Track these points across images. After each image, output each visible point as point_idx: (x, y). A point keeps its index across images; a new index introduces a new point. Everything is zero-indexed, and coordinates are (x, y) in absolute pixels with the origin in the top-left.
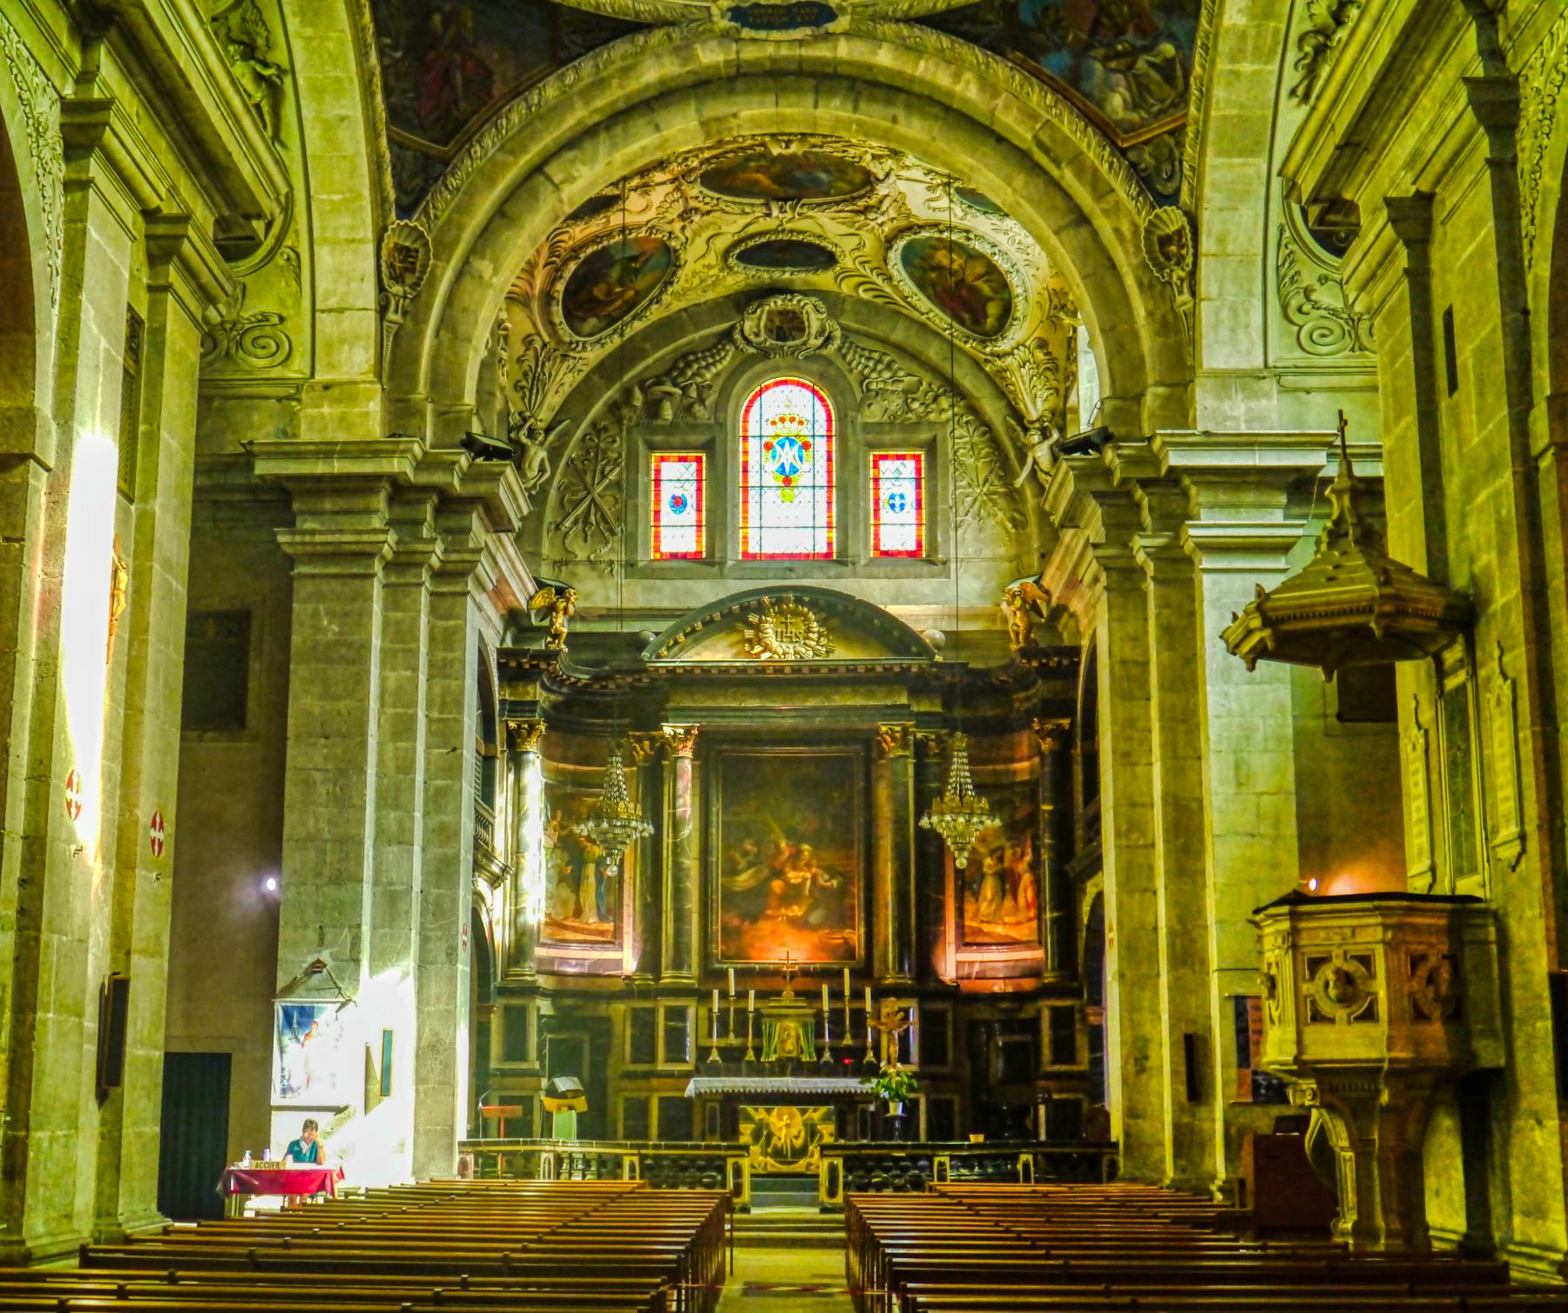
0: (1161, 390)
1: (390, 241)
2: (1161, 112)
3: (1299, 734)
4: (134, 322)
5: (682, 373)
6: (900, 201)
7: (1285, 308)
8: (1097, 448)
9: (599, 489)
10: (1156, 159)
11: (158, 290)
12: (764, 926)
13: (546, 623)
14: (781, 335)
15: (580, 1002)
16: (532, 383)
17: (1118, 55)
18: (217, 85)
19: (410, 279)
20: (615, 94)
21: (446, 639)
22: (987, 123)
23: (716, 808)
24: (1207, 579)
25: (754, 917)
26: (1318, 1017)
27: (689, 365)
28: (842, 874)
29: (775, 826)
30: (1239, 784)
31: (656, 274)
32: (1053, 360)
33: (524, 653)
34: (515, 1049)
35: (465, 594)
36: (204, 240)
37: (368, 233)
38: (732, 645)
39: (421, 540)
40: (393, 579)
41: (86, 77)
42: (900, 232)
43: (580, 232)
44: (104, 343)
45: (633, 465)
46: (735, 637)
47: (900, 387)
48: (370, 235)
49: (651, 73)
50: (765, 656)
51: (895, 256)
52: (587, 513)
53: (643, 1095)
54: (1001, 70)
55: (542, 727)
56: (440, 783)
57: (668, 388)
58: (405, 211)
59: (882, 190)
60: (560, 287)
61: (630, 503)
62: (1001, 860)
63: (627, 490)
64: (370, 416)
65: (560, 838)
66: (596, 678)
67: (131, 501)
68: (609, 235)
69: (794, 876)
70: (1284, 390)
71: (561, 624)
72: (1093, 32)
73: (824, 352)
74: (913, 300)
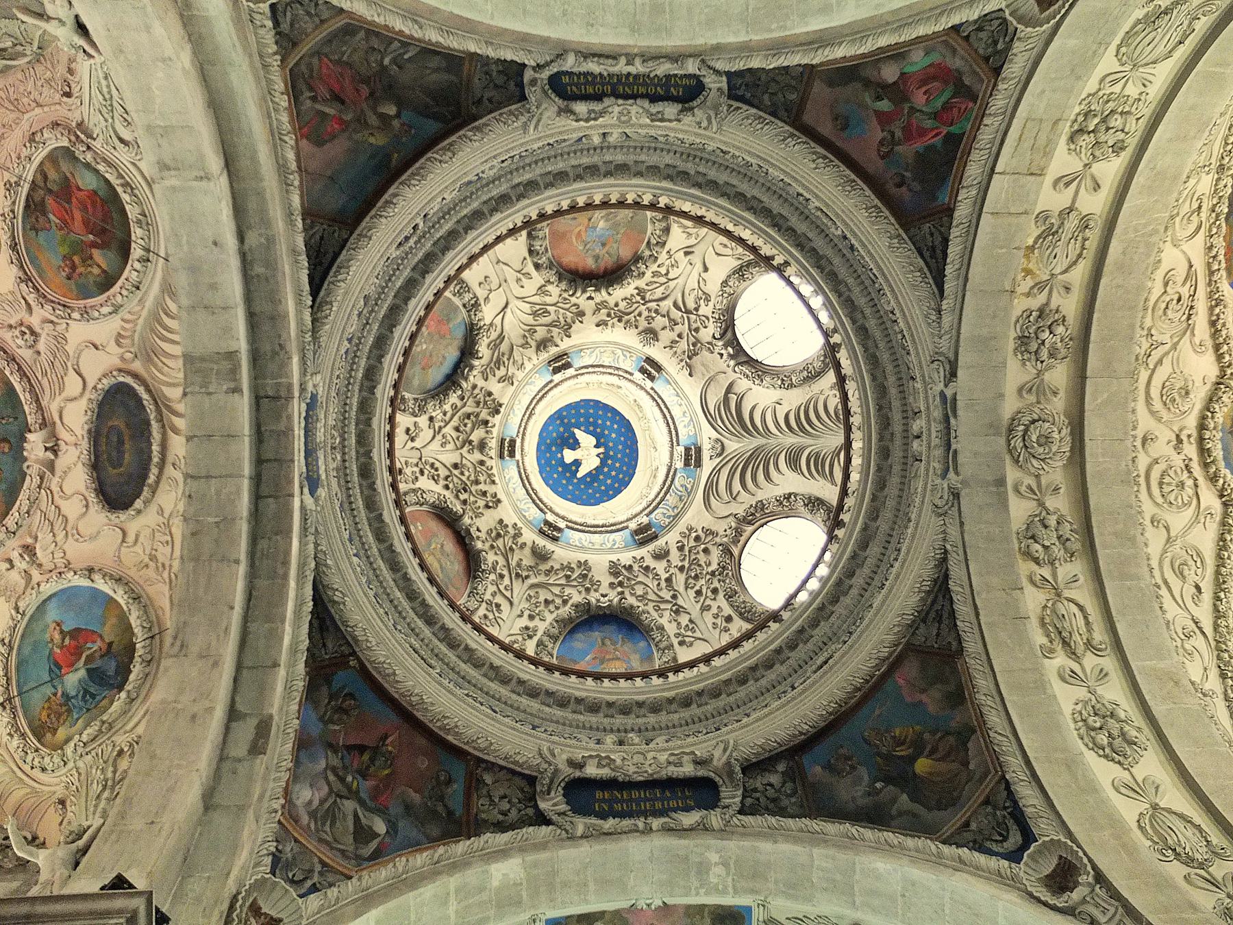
10: (294, 858)
22: (248, 662)
72: (349, 748)
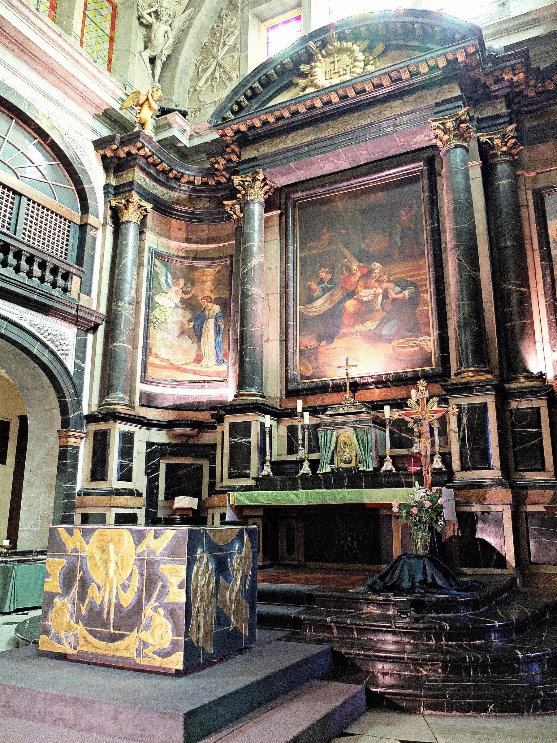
9: (221, 54)
12: (337, 343)
15: (190, 431)
23: (294, 247)
25: (329, 337)
28: (413, 284)
29: (347, 252)
45: (244, 31)
61: (243, 55)
65: (183, 301)
69: (365, 294)
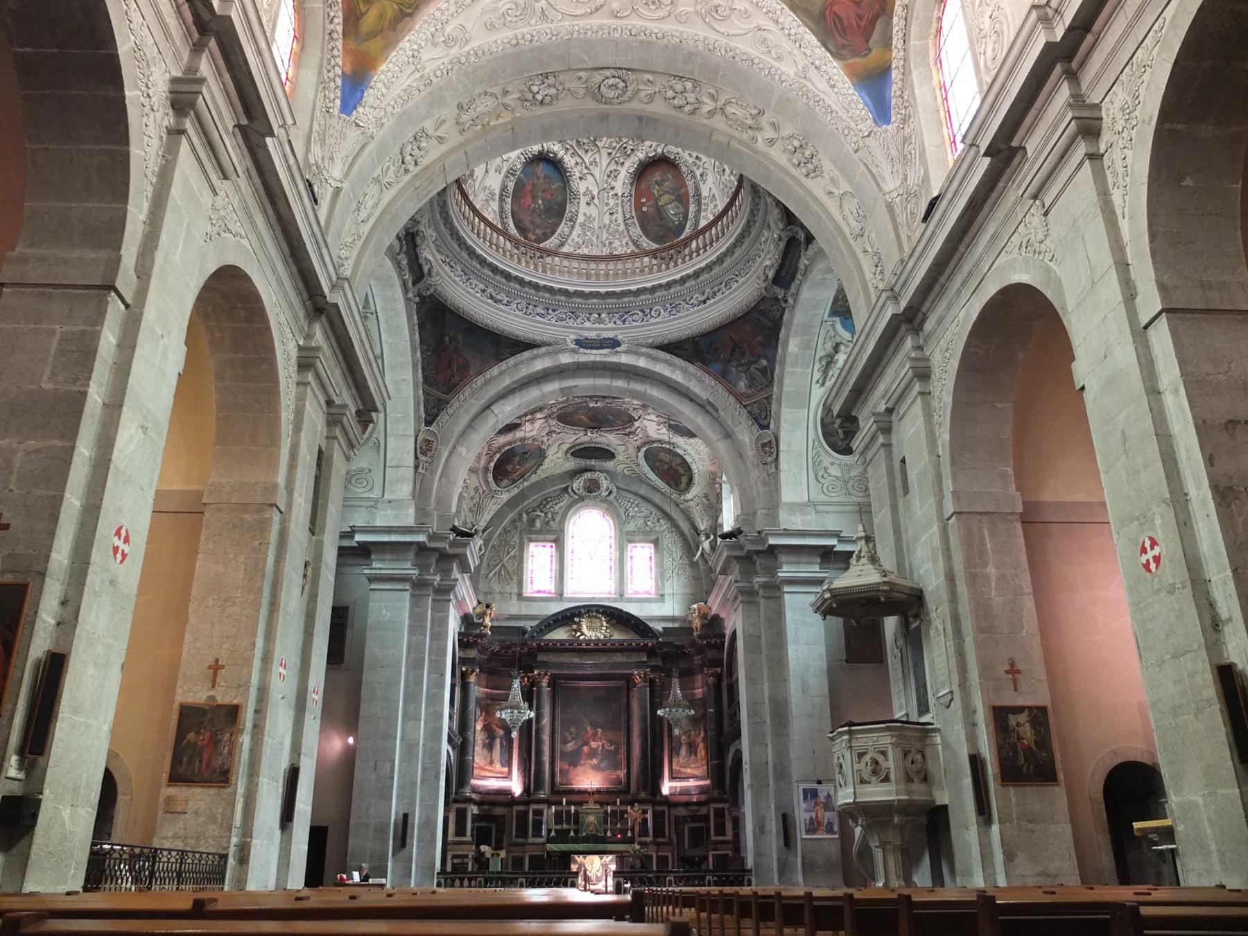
0: (764, 511)
1: (421, 437)
2: (761, 389)
3: (830, 670)
4: (320, 452)
5: (545, 506)
6: (644, 429)
7: (816, 476)
8: (736, 537)
11: (330, 438)
13: (481, 621)
14: (590, 492)
16: (478, 509)
17: (742, 365)
18: (364, 346)
19: (429, 454)
20: (525, 371)
21: (441, 623)
24: (786, 596)
26: (862, 781)
27: (548, 503)
30: (804, 692)
31: (535, 460)
32: (711, 504)
33: (471, 635)
34: (460, 831)
35: (450, 600)
36: (351, 415)
37: (412, 433)
38: (568, 632)
39: (430, 575)
40: (416, 592)
41: (309, 337)
42: (644, 444)
43: (502, 440)
44: (309, 458)
46: (568, 628)
47: (643, 514)
48: (412, 433)
49: (540, 365)
50: (582, 638)
51: (641, 454)
52: (500, 570)
53: (521, 854)
54: (691, 368)
55: (478, 670)
56: (435, 691)
57: (539, 513)
58: (428, 423)
59: (637, 424)
60: (492, 465)
62: (689, 736)
63: (520, 560)
64: (408, 517)
66: (502, 648)
67: (313, 534)
68: (515, 442)
70: (817, 512)
71: (488, 622)
73: (608, 498)
74: (649, 476)
